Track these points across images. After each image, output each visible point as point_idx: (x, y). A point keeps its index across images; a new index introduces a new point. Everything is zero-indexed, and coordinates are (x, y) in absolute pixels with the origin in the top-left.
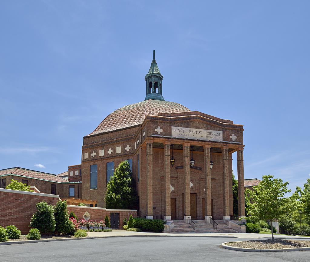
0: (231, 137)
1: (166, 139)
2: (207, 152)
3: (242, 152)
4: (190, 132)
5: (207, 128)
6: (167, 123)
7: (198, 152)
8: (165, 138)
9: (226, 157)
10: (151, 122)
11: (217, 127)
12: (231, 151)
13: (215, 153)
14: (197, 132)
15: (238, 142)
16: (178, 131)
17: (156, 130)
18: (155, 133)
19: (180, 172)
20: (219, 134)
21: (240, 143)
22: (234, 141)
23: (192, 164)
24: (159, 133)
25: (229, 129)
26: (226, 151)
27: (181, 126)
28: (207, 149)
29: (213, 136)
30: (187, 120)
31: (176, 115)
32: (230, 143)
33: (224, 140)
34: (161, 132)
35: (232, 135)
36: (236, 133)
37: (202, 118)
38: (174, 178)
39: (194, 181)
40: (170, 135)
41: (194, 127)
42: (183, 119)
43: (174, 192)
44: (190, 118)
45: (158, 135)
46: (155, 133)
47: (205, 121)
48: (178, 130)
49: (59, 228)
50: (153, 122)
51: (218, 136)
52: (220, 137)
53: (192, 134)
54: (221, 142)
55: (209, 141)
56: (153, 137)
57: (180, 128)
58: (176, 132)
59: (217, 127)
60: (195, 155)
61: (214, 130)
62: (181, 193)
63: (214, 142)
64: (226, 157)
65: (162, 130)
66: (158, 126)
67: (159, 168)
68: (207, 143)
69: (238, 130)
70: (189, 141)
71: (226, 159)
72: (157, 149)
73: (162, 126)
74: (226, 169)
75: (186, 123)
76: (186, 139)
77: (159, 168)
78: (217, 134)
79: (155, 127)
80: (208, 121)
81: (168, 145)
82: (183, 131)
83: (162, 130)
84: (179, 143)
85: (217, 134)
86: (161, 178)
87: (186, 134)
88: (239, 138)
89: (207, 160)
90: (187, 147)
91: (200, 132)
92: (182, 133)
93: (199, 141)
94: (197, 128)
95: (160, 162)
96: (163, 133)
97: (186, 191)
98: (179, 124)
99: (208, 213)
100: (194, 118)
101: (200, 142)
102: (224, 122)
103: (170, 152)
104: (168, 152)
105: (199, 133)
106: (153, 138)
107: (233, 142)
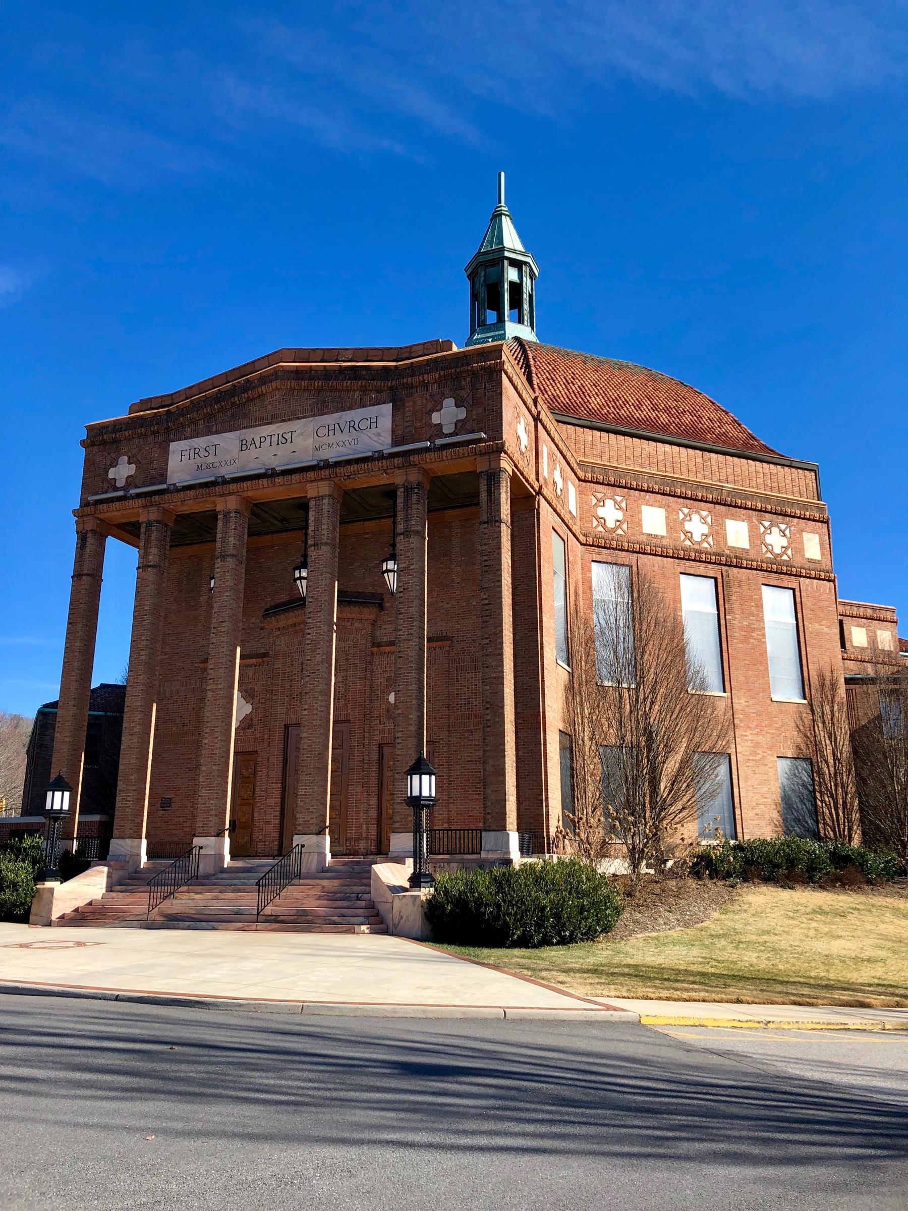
0: (436, 418)
1: (141, 501)
2: (323, 522)
4: (244, 446)
5: (321, 409)
6: (153, 433)
7: (367, 524)
8: (139, 496)
9: (407, 520)
10: (95, 449)
11: (364, 391)
13: (449, 513)
14: (275, 438)
15: (473, 432)
16: (192, 457)
17: (112, 474)
18: (106, 485)
19: (279, 629)
20: (374, 422)
21: (483, 435)
22: (451, 435)
23: (298, 582)
24: (120, 483)
25: (424, 385)
26: (408, 490)
27: (209, 432)
29: (345, 437)
30: (227, 402)
31: (194, 391)
32: (427, 450)
33: (395, 443)
34: (128, 477)
35: (440, 410)
36: (463, 393)
37: (298, 374)
38: (254, 661)
40: (162, 476)
41: (261, 422)
42: (219, 398)
43: (250, 726)
44: (248, 386)
45: (116, 489)
46: (106, 485)
47: (311, 378)
48: (192, 452)
49: (497, 893)
50: (104, 443)
51: (370, 429)
52: (379, 434)
53: (253, 452)
54: (379, 456)
55: (326, 465)
56: (97, 502)
57: (200, 442)
58: (183, 461)
59: (364, 391)
62: (279, 727)
63: (348, 462)
65: (131, 470)
68: (311, 475)
69: (474, 373)
70: (233, 487)
71: (407, 533)
72: (195, 547)
73: (134, 452)
75: (229, 413)
76: (225, 482)
78: (365, 424)
79: (108, 463)
80: (327, 374)
81: (149, 524)
82: (212, 451)
83: (131, 470)
84: (190, 505)
85: (365, 424)
87: (228, 458)
88: (480, 410)
90: (226, 515)
91: (288, 436)
92: (210, 459)
93: (270, 475)
96: (137, 481)
97: (207, 714)
98: (201, 425)
99: (300, 821)
100: (264, 380)
101: (279, 480)
102: (407, 355)
103: (154, 551)
105: (283, 440)
106: (93, 507)
107: (439, 442)
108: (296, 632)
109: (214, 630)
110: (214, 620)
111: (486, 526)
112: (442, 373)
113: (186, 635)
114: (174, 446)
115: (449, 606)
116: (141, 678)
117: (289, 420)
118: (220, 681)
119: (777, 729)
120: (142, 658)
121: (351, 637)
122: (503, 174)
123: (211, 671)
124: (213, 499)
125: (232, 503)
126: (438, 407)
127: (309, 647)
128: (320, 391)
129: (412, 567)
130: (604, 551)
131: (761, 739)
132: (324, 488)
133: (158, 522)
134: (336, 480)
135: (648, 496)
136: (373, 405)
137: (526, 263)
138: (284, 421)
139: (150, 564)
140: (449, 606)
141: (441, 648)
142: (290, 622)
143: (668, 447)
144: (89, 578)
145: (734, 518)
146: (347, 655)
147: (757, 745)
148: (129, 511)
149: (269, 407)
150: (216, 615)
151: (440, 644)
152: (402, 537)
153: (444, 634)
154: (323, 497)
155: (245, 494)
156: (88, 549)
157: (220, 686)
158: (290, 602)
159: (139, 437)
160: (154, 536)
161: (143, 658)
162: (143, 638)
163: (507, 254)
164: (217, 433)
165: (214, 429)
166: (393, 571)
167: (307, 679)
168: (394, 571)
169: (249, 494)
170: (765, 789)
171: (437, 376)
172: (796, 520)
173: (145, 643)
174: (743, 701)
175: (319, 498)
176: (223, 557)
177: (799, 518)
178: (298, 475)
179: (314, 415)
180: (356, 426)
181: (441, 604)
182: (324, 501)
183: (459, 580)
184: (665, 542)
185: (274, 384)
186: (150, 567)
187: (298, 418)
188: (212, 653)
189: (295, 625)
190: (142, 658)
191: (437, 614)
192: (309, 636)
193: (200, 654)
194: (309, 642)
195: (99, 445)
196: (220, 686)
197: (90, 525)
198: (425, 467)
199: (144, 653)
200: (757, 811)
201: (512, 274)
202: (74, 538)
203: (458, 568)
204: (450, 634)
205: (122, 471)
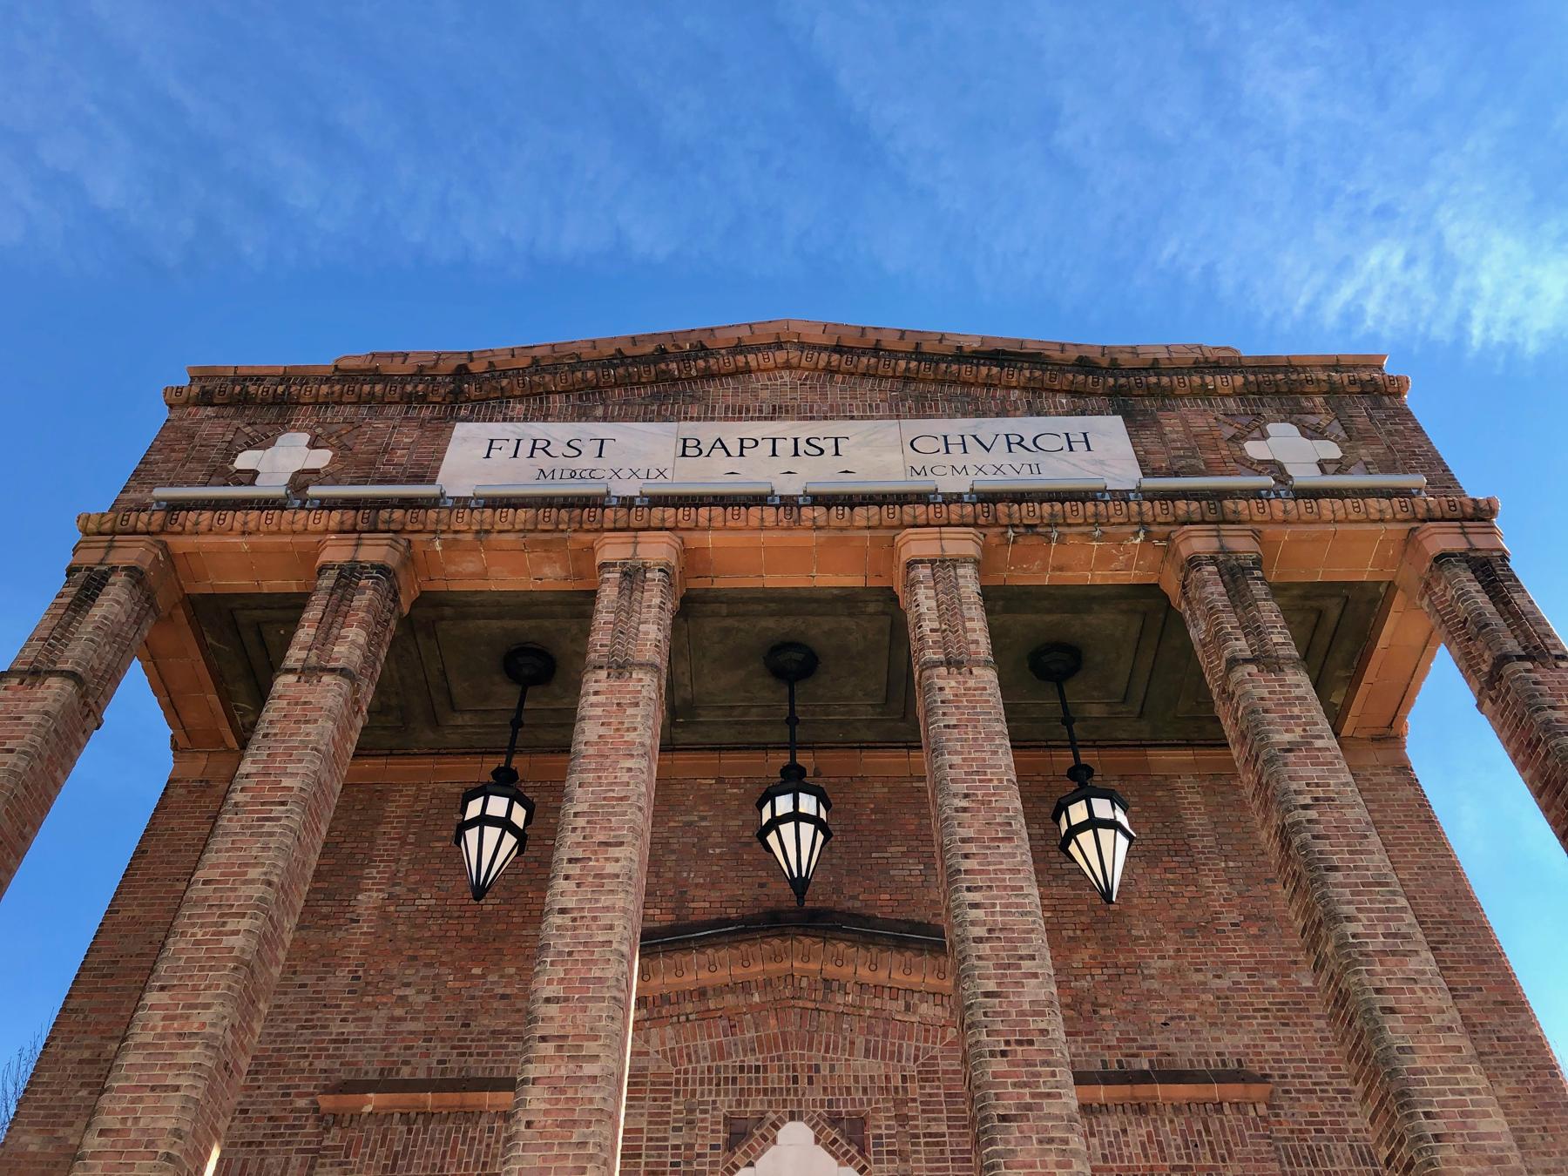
3: (1492, 573)
8: (328, 505)
12: (1339, 636)
28: (923, 572)
39: (882, 1124)
41: (739, 413)
60: (880, 790)
61: (1003, 413)
64: (1253, 629)
66: (284, 425)
67: (342, 976)
74: (1311, 772)
77: (342, 976)
81: (349, 575)
86: (327, 1102)
89: (947, 683)
90: (633, 575)
94: (776, 413)
95: (368, 900)
103: (355, 634)
104: (326, 636)
108: (705, 1015)
109: (568, 869)
110: (571, 838)
111: (1529, 665)
112: (1251, 378)
113: (286, 1000)
114: (461, 429)
115: (1225, 983)
116: (207, 1016)
117: (826, 418)
118: (591, 1047)
120: (228, 941)
121: (909, 1047)
123: (553, 1010)
124: (590, 536)
125: (657, 549)
126: (1256, 434)
127: (985, 949)
128: (907, 379)
129: (1319, 743)
132: (962, 543)
133: (382, 569)
134: (991, 532)
136: (1068, 414)
138: (812, 418)
139: (332, 665)
140: (1225, 983)
141: (1237, 1106)
142: (689, 980)
144: (70, 686)
146: (899, 1103)
148: (287, 539)
149: (765, 394)
150: (581, 822)
151: (1235, 1091)
152: (1253, 669)
153: (1232, 1066)
154: (955, 562)
155: (695, 539)
156: (97, 612)
157: (589, 1069)
158: (672, 930)
159: (359, 402)
160: (362, 600)
161: (237, 942)
162: (253, 873)
164: (605, 419)
165: (599, 412)
166: (1113, 825)
167: (999, 1065)
168: (1113, 825)
169: (710, 539)
171: (1239, 380)
173: (257, 891)
175: (942, 564)
176: (621, 668)
178: (874, 509)
179: (898, 417)
180: (1028, 443)
181: (1199, 977)
182: (960, 571)
183: (1234, 916)
185: (781, 356)
186: (333, 671)
187: (852, 418)
188: (559, 943)
189: (702, 993)
190: (228, 941)
191: (1191, 1005)
192: (979, 914)
193: (320, 1064)
194: (980, 931)
195: (225, 405)
196: (589, 1069)
197: (132, 552)
198: (1267, 529)
199: (245, 924)
202: (52, 585)
203: (1225, 889)
204: (1255, 1068)
205: (283, 459)
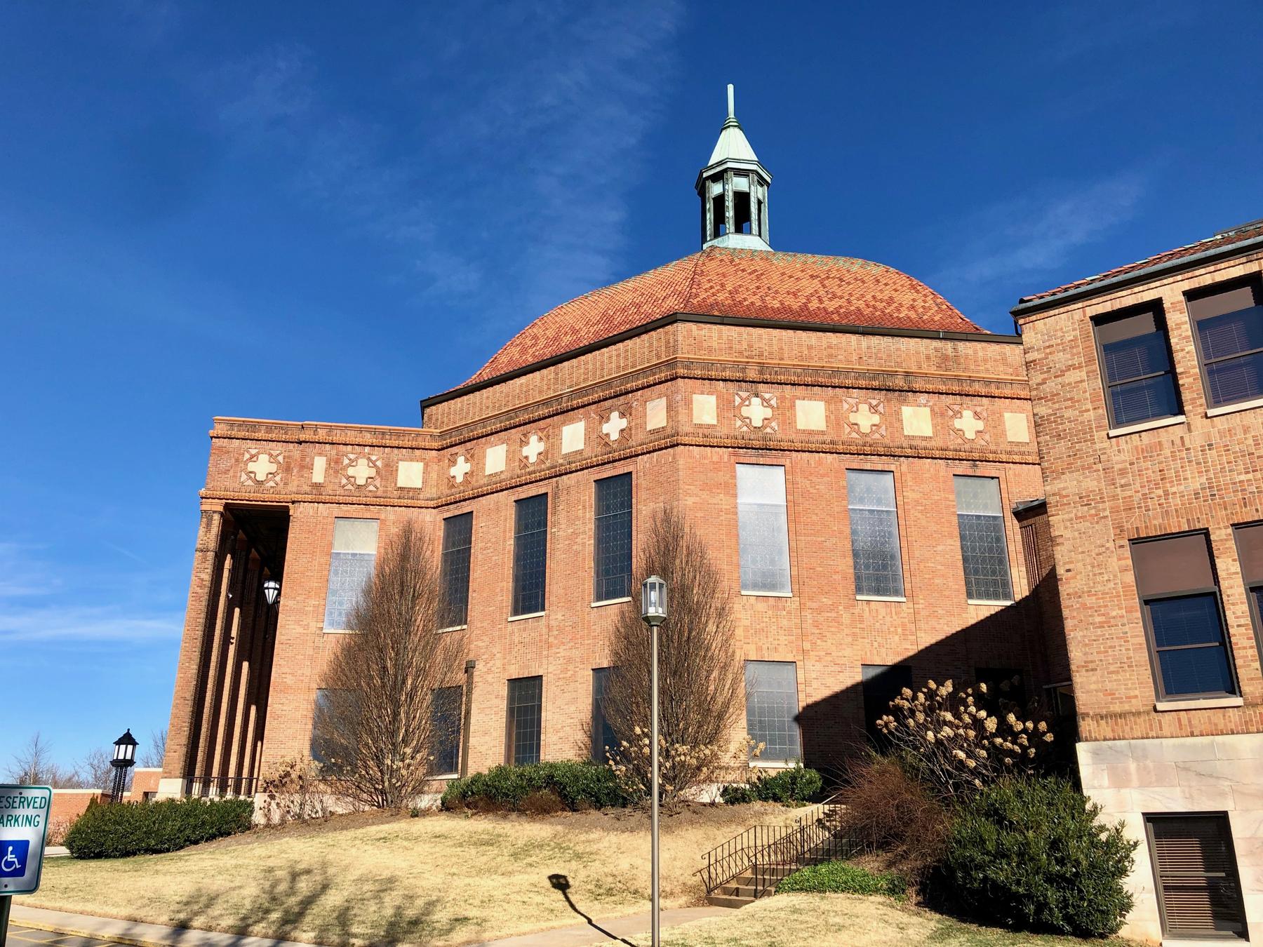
119: (595, 637)
122: (731, 88)
130: (451, 507)
131: (576, 653)
135: (492, 438)
137: (726, 170)
143: (523, 379)
145: (572, 421)
147: (570, 660)
163: (705, 175)
170: (573, 708)
172: (639, 393)
174: (560, 617)
177: (643, 388)
184: (503, 477)
200: (561, 734)
201: (716, 189)
